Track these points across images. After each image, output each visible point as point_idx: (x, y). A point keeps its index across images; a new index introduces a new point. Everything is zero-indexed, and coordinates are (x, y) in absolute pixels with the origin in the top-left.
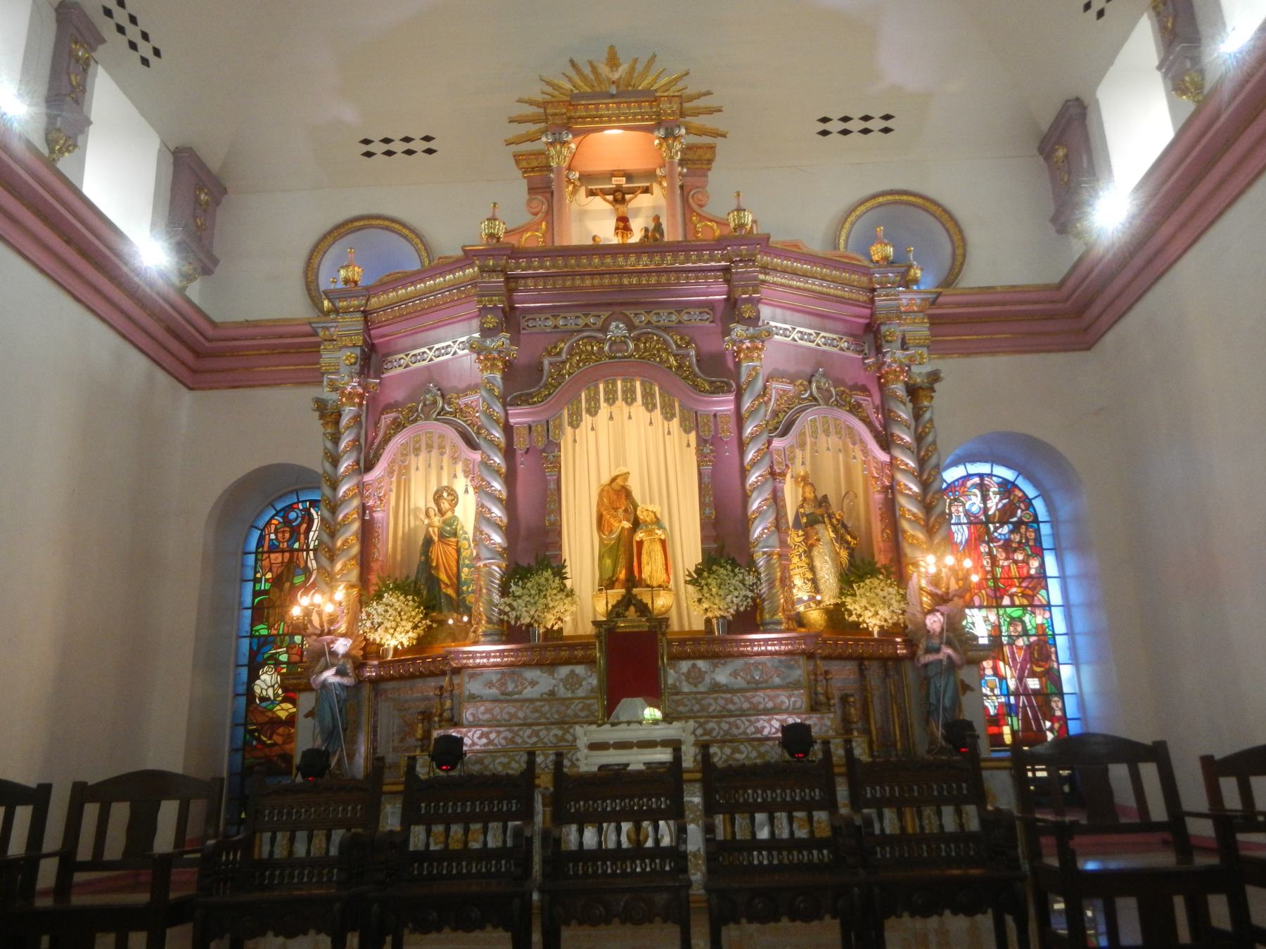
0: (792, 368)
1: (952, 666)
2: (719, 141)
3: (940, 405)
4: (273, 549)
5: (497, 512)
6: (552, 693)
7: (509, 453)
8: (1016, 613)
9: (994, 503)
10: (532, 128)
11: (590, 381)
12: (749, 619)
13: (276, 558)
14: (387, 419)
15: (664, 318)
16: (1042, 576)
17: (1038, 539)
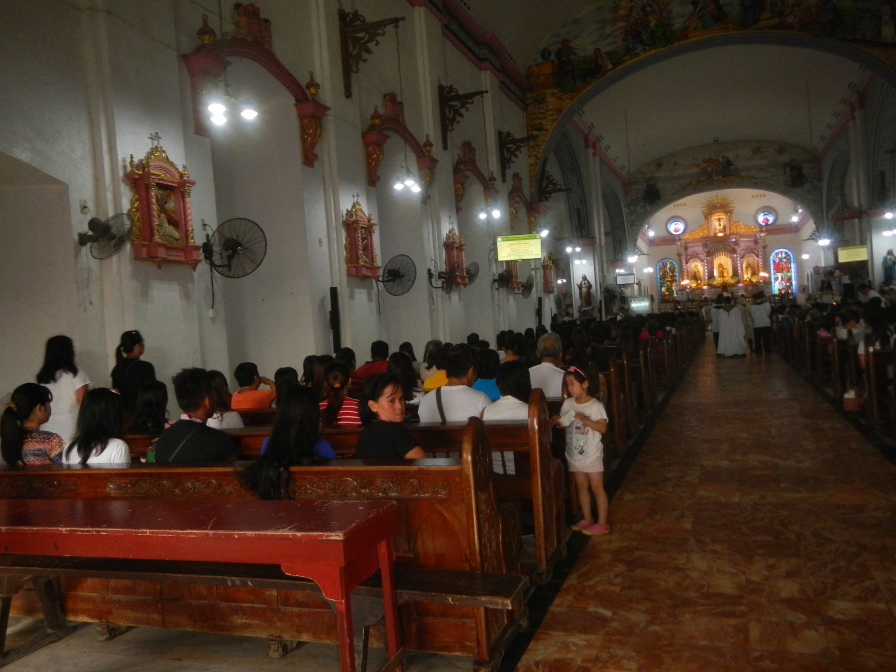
0: (743, 248)
1: (763, 286)
2: (734, 209)
3: (768, 249)
4: (662, 269)
5: (707, 271)
7: (707, 263)
8: (785, 273)
9: (784, 255)
10: (705, 208)
11: (717, 253)
12: (738, 282)
13: (662, 270)
14: (689, 257)
15: (727, 243)
16: (791, 268)
17: (791, 261)
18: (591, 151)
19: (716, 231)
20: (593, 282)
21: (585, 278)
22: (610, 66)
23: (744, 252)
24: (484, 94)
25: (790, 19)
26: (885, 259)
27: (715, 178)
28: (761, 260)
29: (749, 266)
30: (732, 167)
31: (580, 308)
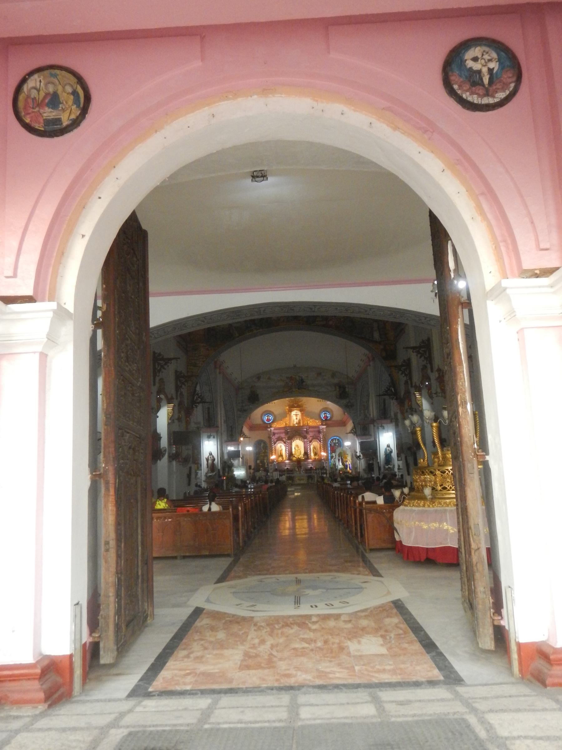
0: (312, 436)
5: (287, 450)
6: (293, 465)
9: (337, 441)
18: (218, 371)
19: (294, 423)
20: (216, 457)
21: (211, 454)
22: (237, 335)
23: (312, 438)
24: (178, 360)
25: (331, 323)
26: (386, 450)
27: (294, 390)
28: (322, 444)
29: (314, 448)
30: (304, 383)
31: (206, 473)
